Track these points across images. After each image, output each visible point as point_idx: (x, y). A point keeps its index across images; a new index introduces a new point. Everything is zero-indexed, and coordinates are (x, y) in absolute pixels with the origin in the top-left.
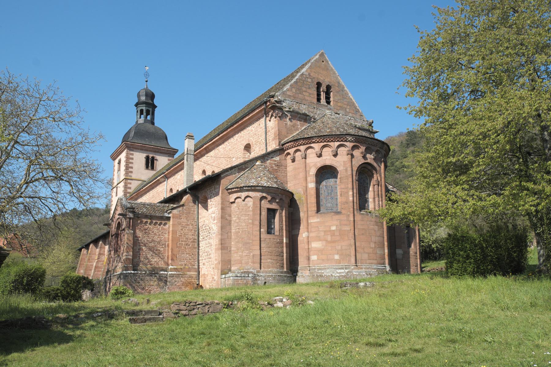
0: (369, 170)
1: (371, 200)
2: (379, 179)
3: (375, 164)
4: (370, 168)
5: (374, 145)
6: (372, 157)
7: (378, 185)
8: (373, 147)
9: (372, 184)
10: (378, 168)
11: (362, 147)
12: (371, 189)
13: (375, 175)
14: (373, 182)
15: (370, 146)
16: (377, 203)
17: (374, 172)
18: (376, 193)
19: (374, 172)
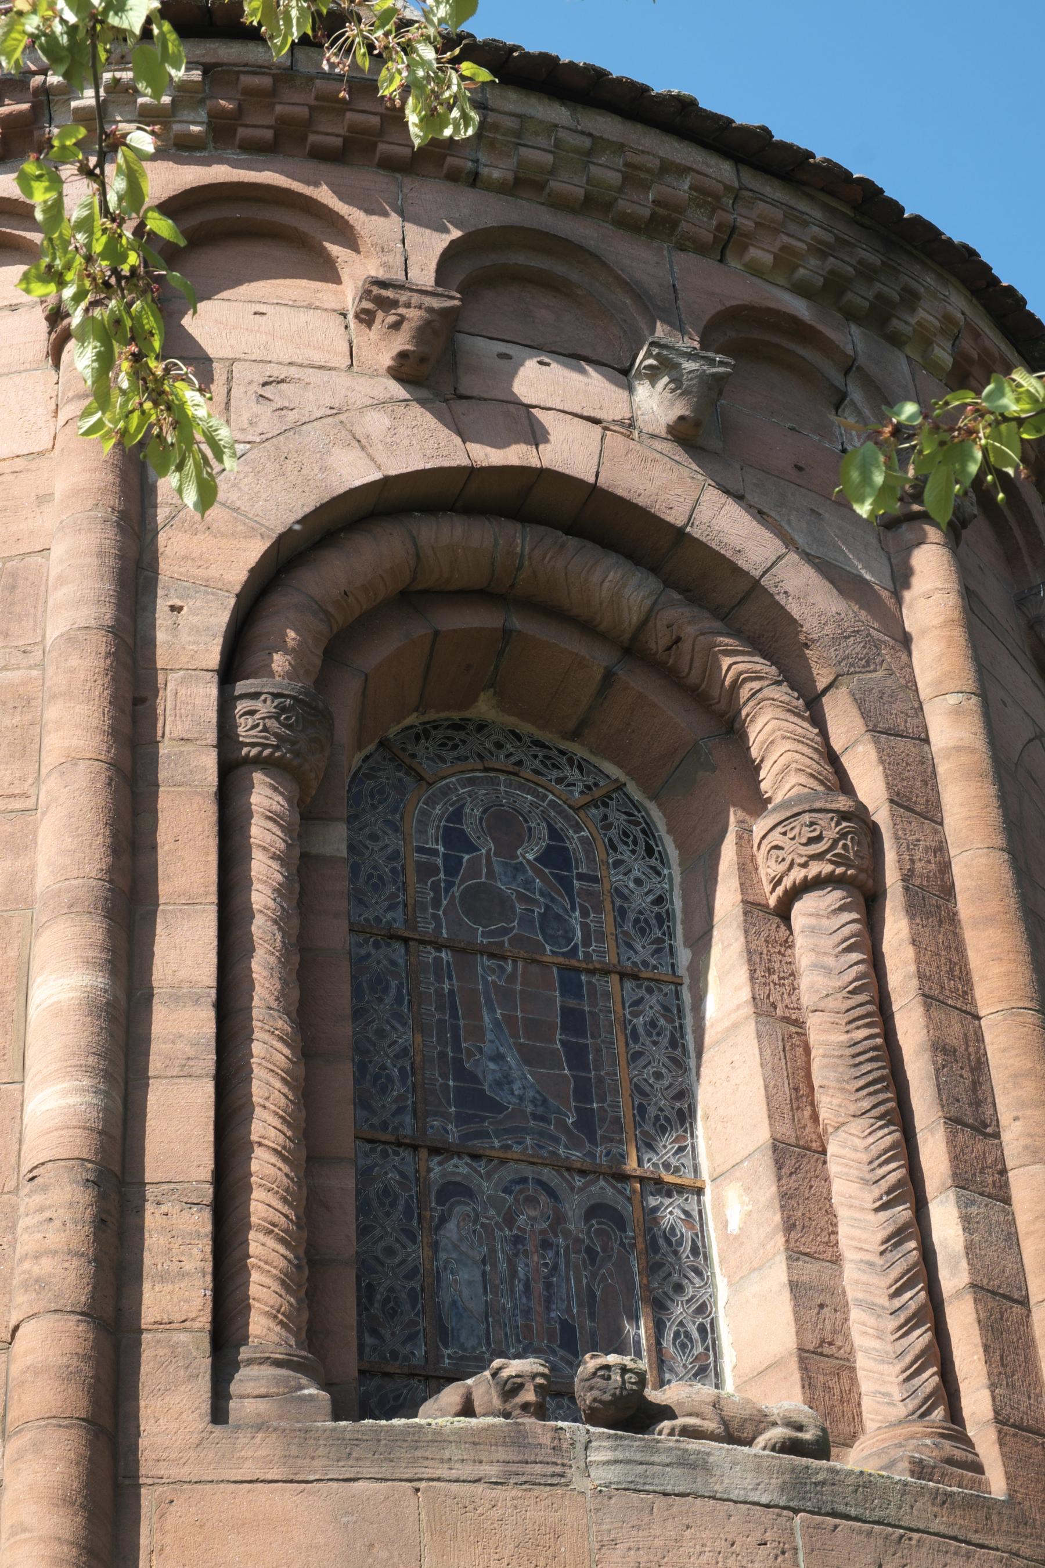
0: (633, 649)
1: (733, 1206)
2: (870, 784)
3: (730, 527)
4: (622, 590)
5: (659, 226)
6: (654, 403)
7: (869, 902)
8: (641, 260)
9: (727, 898)
10: (806, 596)
11: (377, 228)
12: (726, 992)
13: (773, 736)
14: (753, 855)
15: (583, 230)
16: (860, 1226)
17: (734, 664)
18: (828, 1038)
19: (734, 664)
